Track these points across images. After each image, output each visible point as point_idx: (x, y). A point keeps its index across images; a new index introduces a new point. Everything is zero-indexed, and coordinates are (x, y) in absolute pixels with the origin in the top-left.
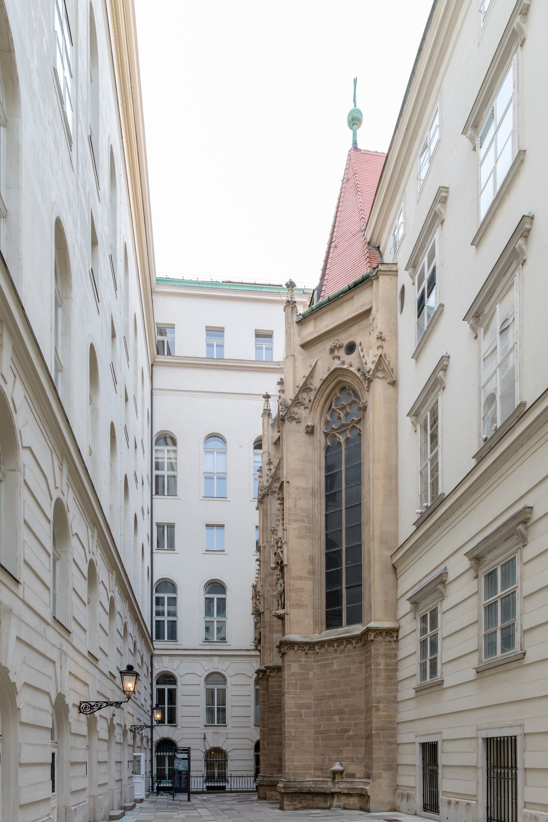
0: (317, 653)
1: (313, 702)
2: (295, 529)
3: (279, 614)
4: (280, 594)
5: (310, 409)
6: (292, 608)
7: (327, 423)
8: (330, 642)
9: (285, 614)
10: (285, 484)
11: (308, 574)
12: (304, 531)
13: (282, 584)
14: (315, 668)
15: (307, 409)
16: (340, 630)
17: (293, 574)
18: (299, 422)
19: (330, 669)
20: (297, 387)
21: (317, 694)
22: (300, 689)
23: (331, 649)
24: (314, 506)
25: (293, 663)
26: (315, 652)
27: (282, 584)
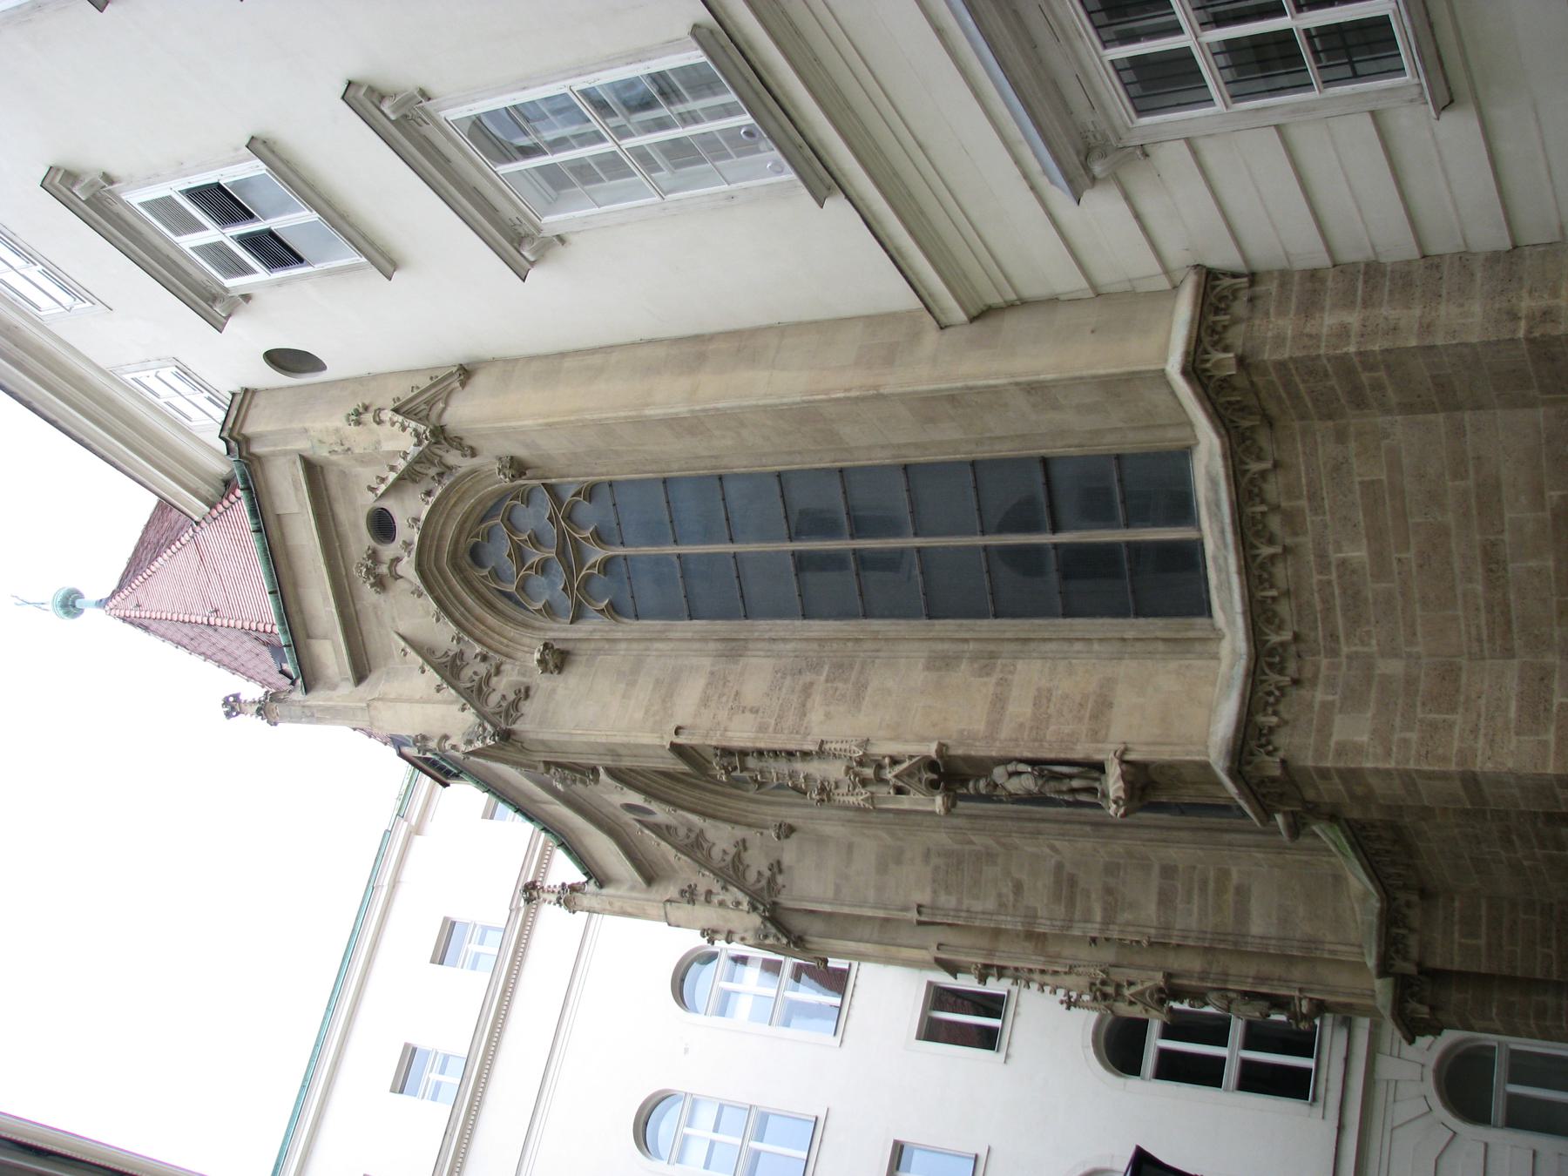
0: (1297, 637)
1: (1516, 662)
2: (828, 715)
3: (1121, 784)
4: (1047, 781)
5: (504, 659)
6: (1107, 734)
7: (549, 611)
8: (1254, 573)
9: (1123, 762)
10: (681, 740)
11: (988, 674)
12: (840, 685)
13: (1011, 768)
14: (1360, 649)
15: (503, 668)
16: (1210, 548)
17: (980, 727)
18: (527, 690)
19: (1369, 579)
20: (438, 691)
21: (1480, 640)
22: (1453, 710)
23: (1281, 573)
24: (769, 653)
25: (1331, 735)
26: (1293, 649)
27: (1011, 768)
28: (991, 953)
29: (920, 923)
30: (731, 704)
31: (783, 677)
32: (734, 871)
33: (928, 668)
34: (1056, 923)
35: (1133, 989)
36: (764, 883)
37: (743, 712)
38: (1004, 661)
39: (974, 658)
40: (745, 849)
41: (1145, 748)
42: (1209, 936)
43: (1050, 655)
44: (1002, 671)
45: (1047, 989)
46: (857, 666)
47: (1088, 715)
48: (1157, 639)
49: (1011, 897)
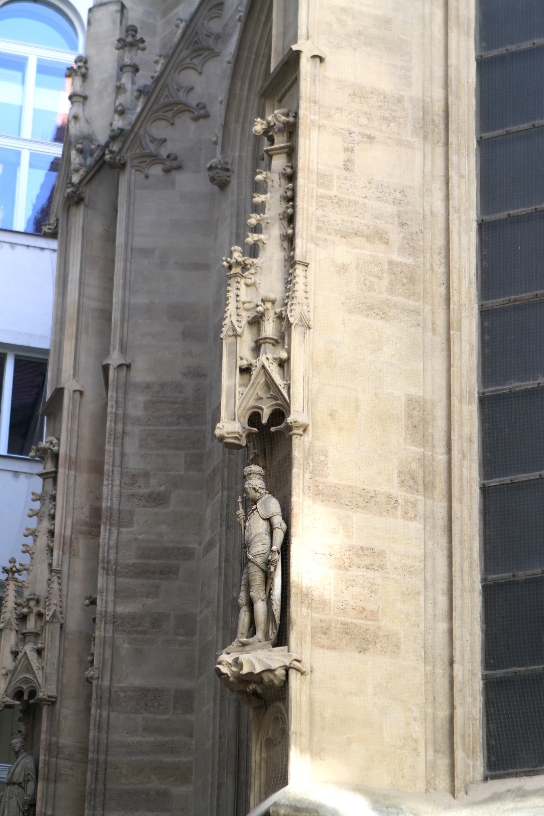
2: (343, 268)
6: (323, 647)
13: (278, 521)
28: (72, 464)
29: (106, 368)
30: (356, 130)
31: (397, 202)
32: (166, 105)
33: (410, 401)
34: (113, 551)
35: (33, 656)
36: (152, 148)
37: (346, 150)
38: (420, 506)
39: (423, 461)
40: (196, 119)
41: (304, 698)
42: (102, 758)
43: (429, 563)
44: (407, 501)
45: (29, 540)
46: (411, 303)
47: (349, 620)
48: (452, 707)
49: (144, 491)
